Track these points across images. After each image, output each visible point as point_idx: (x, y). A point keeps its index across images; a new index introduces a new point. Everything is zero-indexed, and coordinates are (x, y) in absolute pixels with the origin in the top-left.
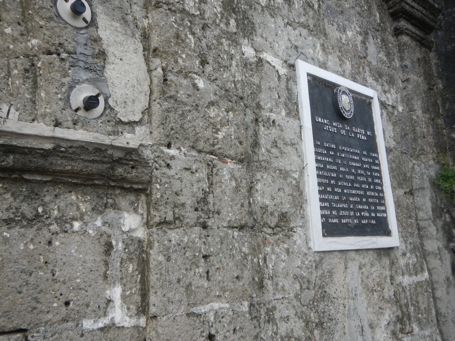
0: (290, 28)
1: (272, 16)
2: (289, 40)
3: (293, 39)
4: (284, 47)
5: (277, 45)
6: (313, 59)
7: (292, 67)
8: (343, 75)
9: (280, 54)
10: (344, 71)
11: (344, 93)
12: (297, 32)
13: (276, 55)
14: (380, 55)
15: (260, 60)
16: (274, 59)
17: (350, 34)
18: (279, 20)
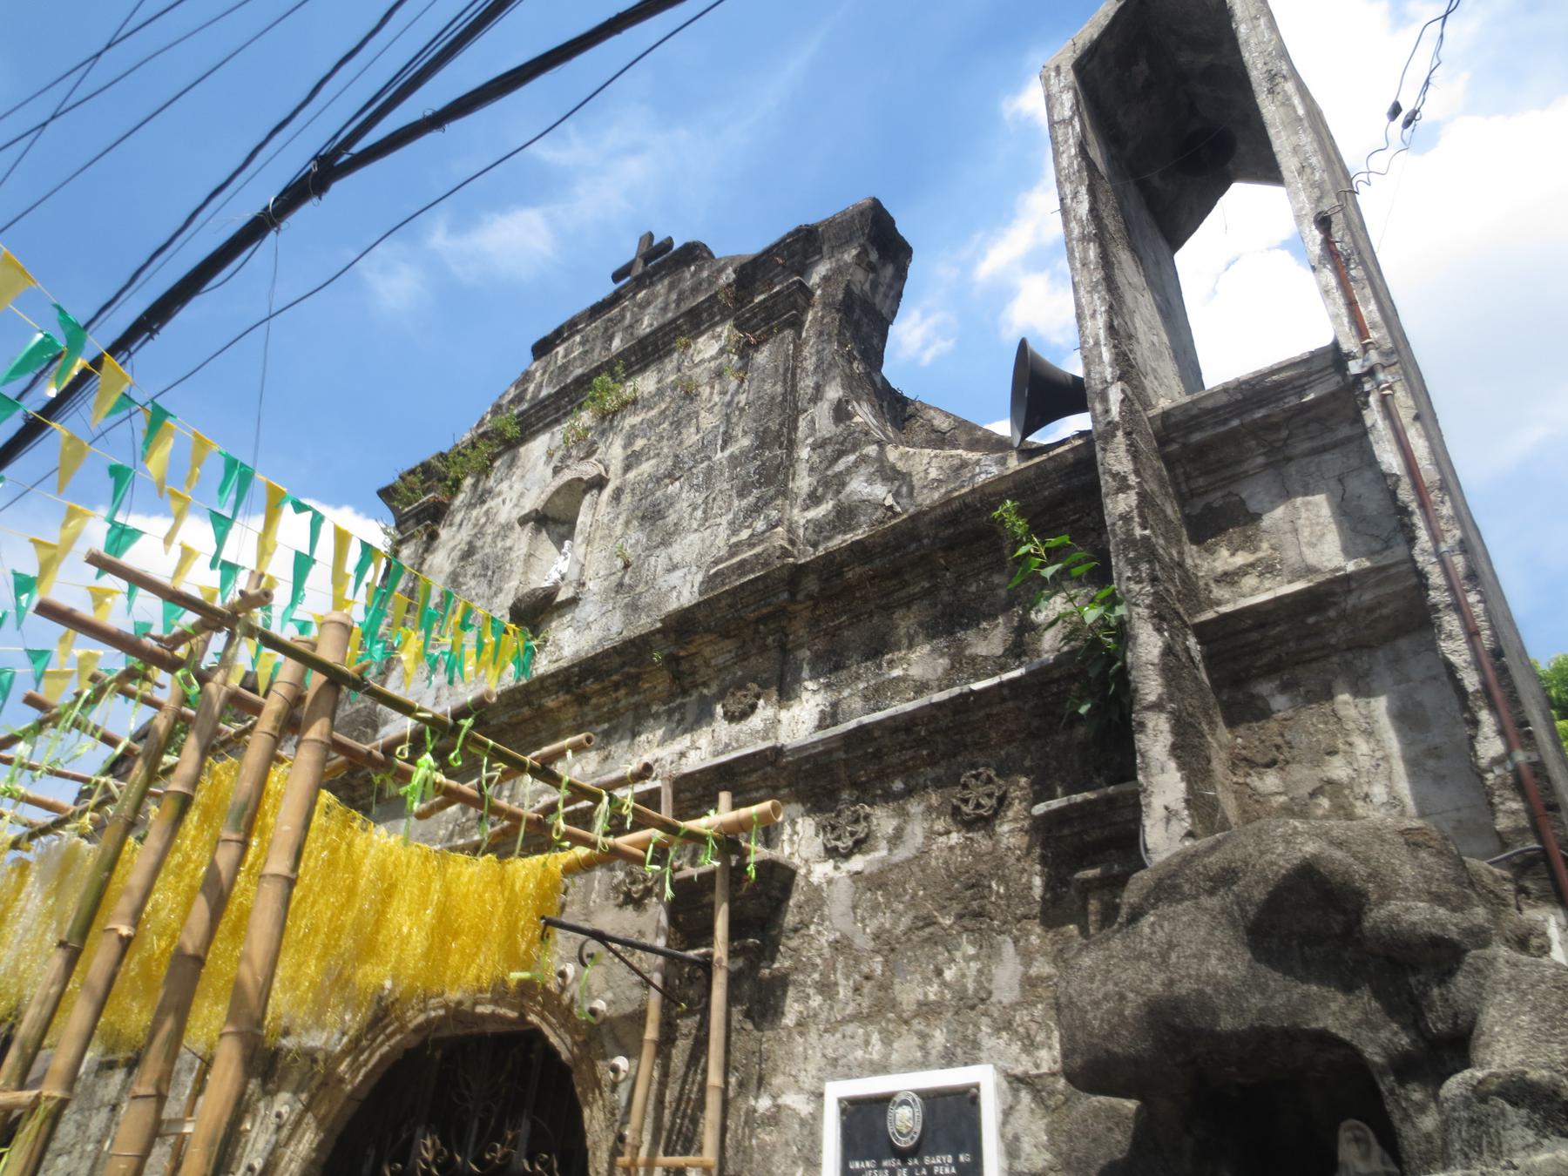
0: (827, 1035)
1: (801, 1034)
2: (824, 1056)
3: (829, 1052)
4: (814, 1072)
5: (803, 1073)
6: (860, 1066)
7: (820, 1096)
8: (924, 1065)
9: (806, 1086)
10: (927, 1054)
11: (905, 1103)
12: (838, 1035)
13: (800, 1090)
14: (1033, 972)
15: (778, 1107)
16: (796, 1097)
17: (949, 975)
18: (813, 1036)
